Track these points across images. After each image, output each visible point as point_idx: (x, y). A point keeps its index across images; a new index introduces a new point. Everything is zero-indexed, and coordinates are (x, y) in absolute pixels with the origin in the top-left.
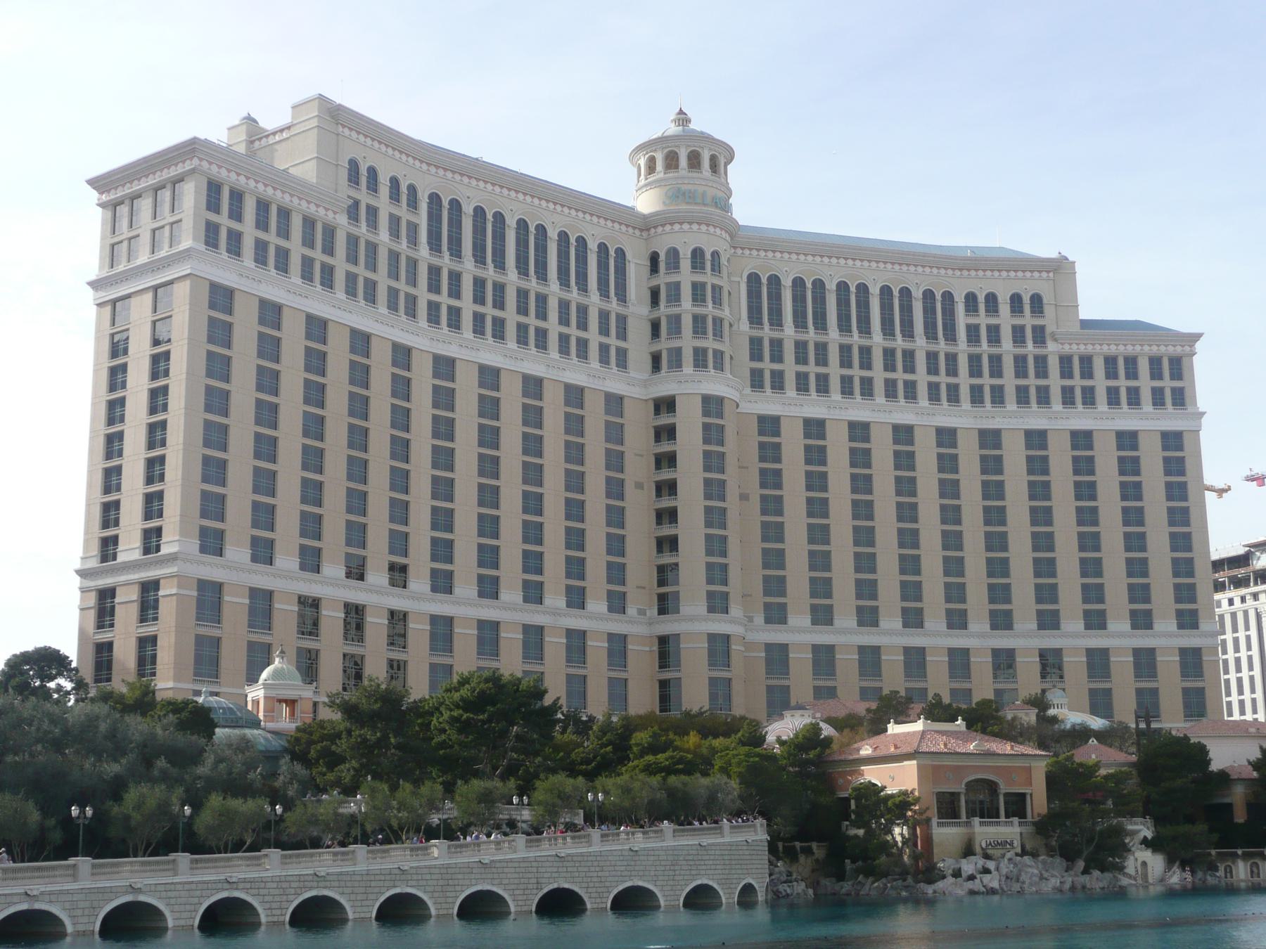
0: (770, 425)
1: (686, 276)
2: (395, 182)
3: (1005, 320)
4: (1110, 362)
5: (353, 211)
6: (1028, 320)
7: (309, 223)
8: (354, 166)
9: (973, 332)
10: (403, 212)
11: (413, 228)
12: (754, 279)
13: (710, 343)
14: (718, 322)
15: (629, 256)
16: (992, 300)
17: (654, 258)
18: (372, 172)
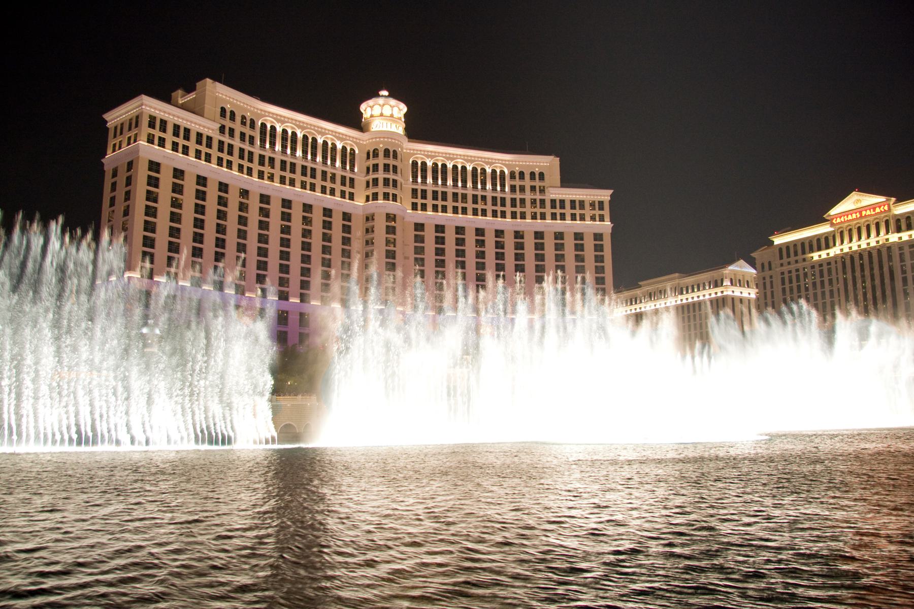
0: (419, 227)
1: (381, 161)
2: (243, 117)
3: (527, 183)
4: (573, 202)
5: (222, 129)
7: (199, 135)
8: (223, 110)
9: (513, 189)
11: (252, 139)
12: (415, 164)
13: (391, 190)
14: (395, 182)
15: (357, 152)
16: (522, 174)
17: (368, 154)
18: (233, 114)
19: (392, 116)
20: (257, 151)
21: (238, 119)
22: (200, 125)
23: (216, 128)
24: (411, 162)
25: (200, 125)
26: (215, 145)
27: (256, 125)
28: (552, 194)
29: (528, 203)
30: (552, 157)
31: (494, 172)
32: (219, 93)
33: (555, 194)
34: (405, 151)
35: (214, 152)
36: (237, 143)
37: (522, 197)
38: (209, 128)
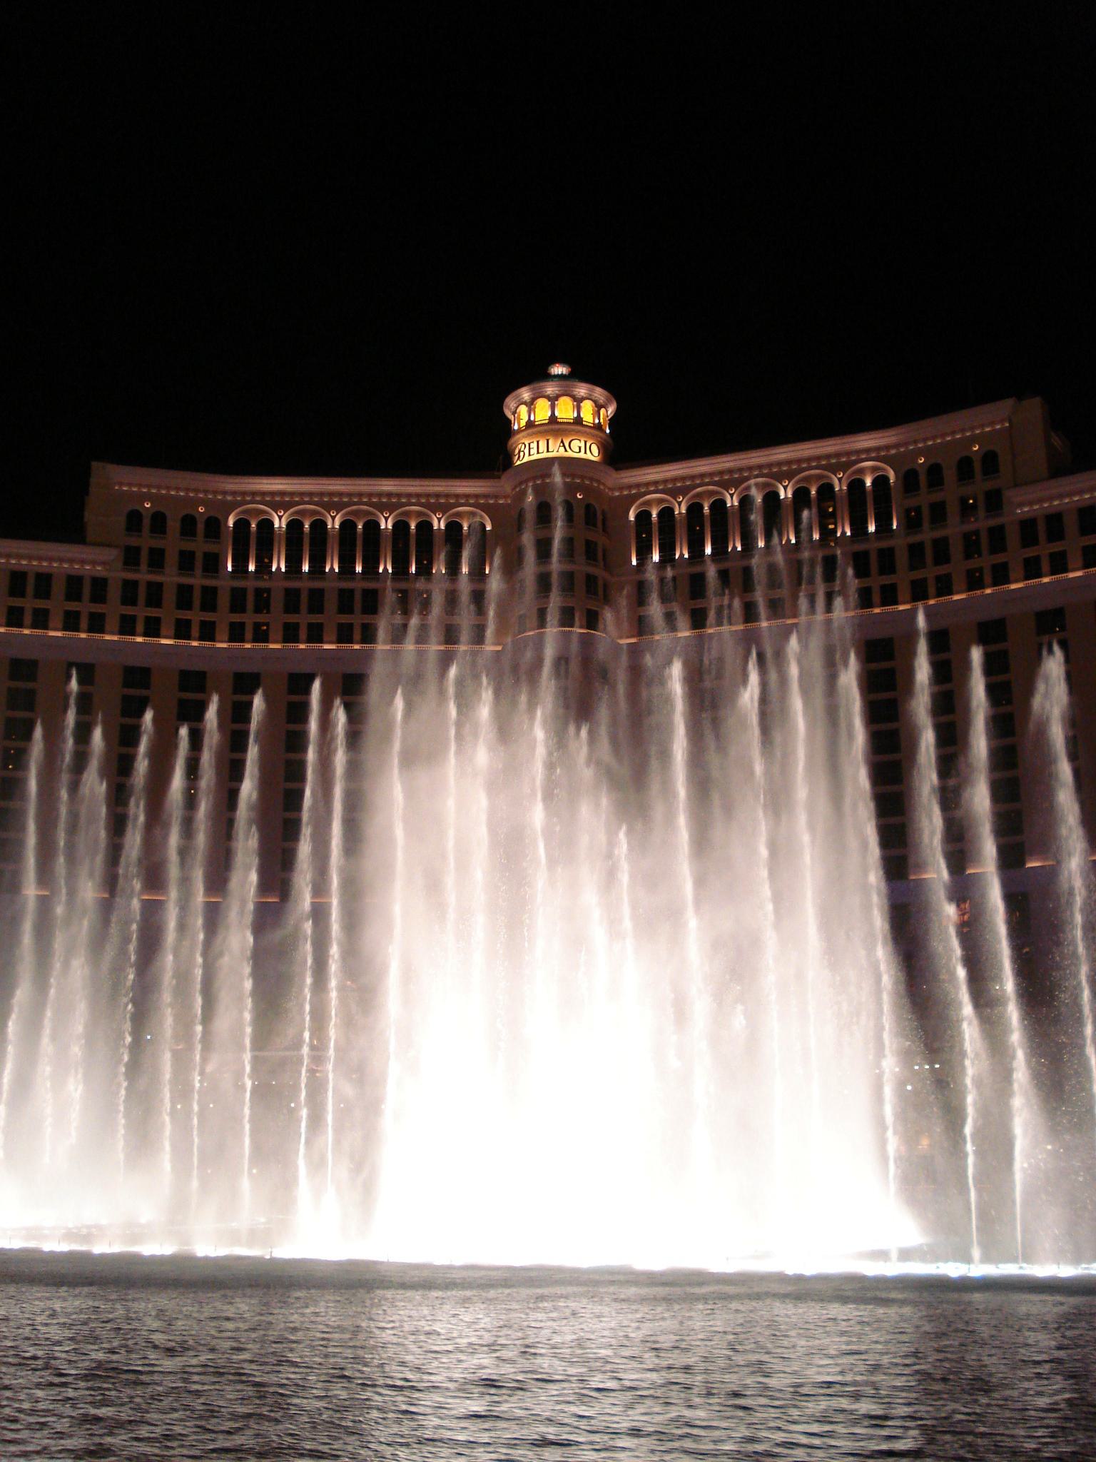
5: (131, 557)
6: (981, 485)
8: (134, 520)
10: (200, 546)
12: (644, 516)
15: (489, 528)
19: (553, 419)
20: (224, 585)
21: (174, 525)
22: (71, 561)
23: (112, 557)
24: (632, 517)
25: (71, 561)
26: (114, 593)
27: (223, 528)
28: (1021, 505)
29: (956, 550)
30: (1005, 406)
31: (856, 485)
32: (121, 484)
33: (1031, 503)
34: (617, 494)
35: (113, 608)
36: (170, 577)
37: (938, 534)
38: (94, 563)
